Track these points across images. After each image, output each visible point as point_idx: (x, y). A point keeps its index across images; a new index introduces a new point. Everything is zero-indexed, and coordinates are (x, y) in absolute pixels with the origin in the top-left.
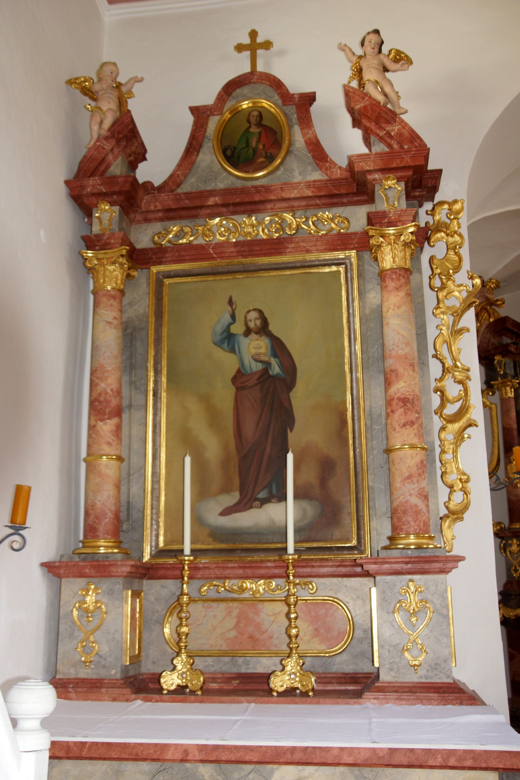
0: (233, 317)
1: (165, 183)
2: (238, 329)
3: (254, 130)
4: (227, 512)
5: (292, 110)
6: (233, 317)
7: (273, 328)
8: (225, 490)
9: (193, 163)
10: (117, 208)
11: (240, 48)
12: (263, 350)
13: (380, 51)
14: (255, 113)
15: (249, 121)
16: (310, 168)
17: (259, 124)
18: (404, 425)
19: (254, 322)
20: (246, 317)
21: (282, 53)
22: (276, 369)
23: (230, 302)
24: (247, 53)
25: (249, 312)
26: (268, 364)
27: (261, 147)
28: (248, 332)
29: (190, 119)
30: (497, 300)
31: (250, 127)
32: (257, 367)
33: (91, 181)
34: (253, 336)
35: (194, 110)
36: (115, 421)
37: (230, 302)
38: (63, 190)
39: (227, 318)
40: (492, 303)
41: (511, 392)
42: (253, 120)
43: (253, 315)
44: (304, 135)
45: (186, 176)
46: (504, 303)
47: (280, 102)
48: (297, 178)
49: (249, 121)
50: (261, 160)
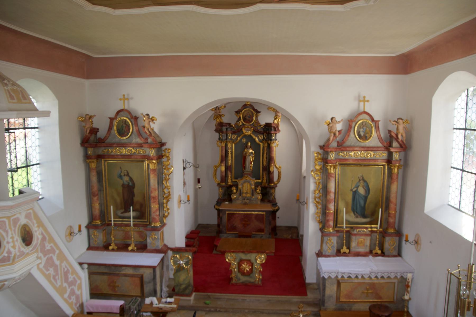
0: (121, 171)
1: (104, 139)
2: (122, 174)
3: (124, 125)
4: (122, 213)
5: (133, 120)
6: (121, 171)
7: (130, 175)
8: (121, 209)
9: (110, 133)
10: (92, 148)
11: (121, 99)
12: (128, 180)
13: (149, 117)
14: (124, 121)
15: (123, 123)
16: (137, 137)
17: (125, 124)
18: (153, 202)
19: (126, 173)
20: (124, 172)
21: (132, 98)
22: (131, 184)
23: (120, 168)
24: (122, 101)
25: (125, 170)
26: (129, 183)
27: (126, 130)
28: (125, 175)
29: (109, 120)
30: (223, 115)
31: (123, 124)
32: (127, 183)
33: (86, 144)
34: (126, 176)
35: (110, 118)
36: (97, 197)
37: (120, 168)
38: (79, 145)
39: (120, 172)
40: (221, 116)
41: (224, 144)
42: (124, 122)
43: (125, 171)
44: (136, 128)
45: (109, 137)
46: (224, 115)
47: (130, 118)
48: (134, 141)
49: (123, 123)
50: (126, 134)
